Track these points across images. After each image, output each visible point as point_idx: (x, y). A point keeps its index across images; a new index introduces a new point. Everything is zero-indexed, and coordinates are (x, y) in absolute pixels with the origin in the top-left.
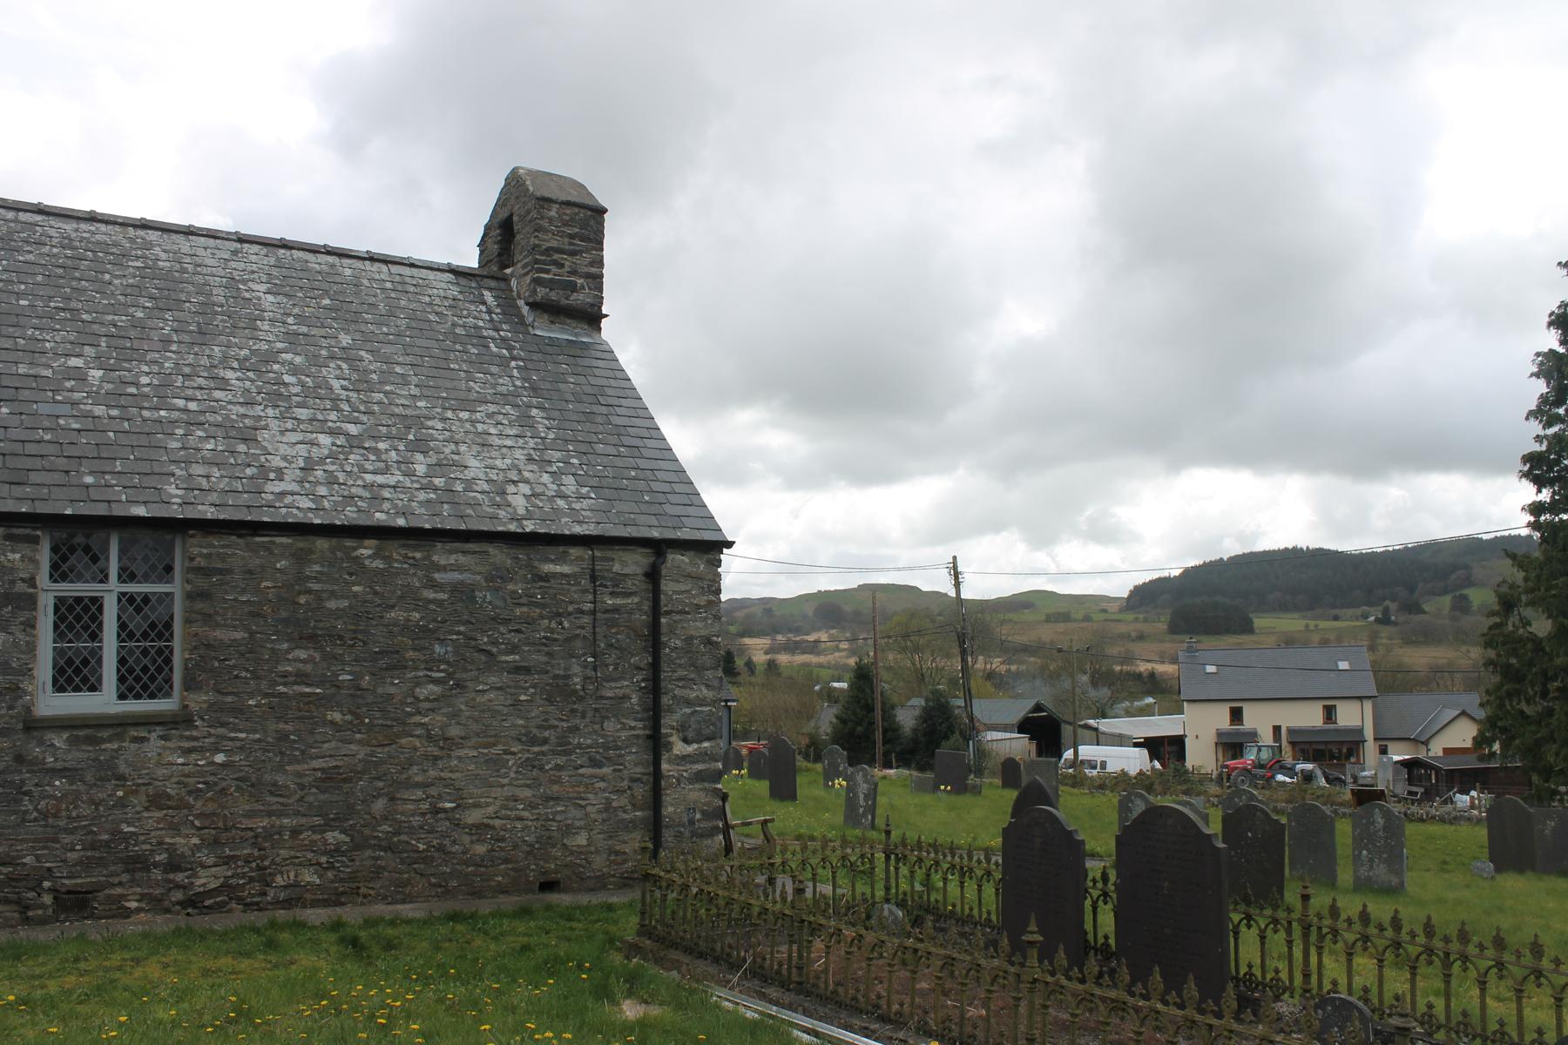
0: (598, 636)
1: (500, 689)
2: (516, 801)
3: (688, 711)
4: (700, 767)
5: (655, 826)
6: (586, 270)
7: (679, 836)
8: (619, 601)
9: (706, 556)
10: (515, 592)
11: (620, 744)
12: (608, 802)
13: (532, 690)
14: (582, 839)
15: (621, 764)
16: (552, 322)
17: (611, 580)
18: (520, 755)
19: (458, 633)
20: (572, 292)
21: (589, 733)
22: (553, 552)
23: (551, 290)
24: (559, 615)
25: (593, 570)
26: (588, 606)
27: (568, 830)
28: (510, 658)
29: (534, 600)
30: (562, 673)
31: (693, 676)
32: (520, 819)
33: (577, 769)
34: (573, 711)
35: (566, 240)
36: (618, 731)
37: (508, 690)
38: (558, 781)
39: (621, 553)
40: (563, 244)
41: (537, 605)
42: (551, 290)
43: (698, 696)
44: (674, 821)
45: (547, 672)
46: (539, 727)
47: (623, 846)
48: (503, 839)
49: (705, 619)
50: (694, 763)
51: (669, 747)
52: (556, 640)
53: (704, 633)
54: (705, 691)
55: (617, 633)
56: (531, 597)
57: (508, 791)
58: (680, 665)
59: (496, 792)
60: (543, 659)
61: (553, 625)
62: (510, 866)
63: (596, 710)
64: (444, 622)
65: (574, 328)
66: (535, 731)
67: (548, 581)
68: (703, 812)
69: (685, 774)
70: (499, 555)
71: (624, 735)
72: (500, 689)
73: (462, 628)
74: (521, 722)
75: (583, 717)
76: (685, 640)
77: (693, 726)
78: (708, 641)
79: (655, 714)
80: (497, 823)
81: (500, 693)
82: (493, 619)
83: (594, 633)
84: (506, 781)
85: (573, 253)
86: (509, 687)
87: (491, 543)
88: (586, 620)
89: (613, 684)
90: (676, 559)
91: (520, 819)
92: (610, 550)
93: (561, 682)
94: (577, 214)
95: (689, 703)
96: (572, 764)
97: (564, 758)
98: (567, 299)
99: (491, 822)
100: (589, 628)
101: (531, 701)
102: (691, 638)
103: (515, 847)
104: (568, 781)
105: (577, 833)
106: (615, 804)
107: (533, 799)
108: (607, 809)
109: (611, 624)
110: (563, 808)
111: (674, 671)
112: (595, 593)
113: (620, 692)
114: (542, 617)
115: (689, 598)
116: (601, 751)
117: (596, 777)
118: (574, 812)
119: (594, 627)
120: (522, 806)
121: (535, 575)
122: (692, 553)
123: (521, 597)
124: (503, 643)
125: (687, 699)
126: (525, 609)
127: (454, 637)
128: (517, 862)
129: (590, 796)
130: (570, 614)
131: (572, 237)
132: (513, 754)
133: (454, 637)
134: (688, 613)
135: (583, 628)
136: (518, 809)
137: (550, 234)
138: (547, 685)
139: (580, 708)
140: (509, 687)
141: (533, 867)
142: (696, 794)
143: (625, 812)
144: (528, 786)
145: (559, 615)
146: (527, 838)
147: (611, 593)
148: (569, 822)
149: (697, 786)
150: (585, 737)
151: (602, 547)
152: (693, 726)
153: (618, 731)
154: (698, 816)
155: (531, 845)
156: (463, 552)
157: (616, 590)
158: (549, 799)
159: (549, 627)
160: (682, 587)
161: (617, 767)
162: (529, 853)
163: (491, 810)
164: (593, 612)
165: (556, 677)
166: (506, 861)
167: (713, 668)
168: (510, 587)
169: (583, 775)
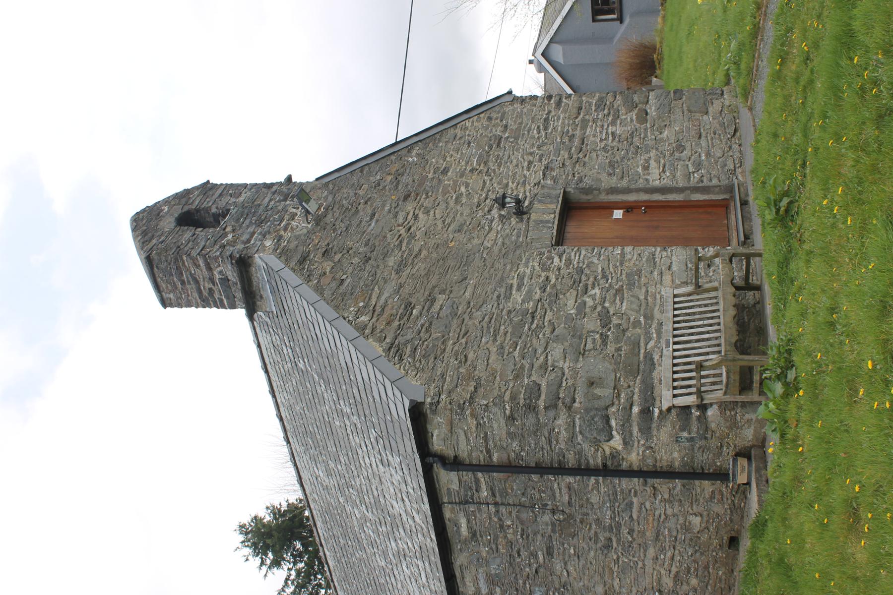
0: (517, 502)
1: (566, 564)
2: (657, 559)
3: (580, 437)
4: (635, 430)
5: (690, 474)
6: (204, 270)
7: (703, 449)
8: (483, 486)
9: (429, 416)
10: (488, 552)
11: (611, 492)
12: (663, 500)
13: (566, 545)
14: (696, 521)
15: (630, 491)
16: (261, 297)
17: (466, 491)
18: (620, 554)
19: (525, 583)
20: (228, 280)
21: (601, 512)
22: (450, 529)
23: (235, 297)
24: (501, 527)
25: (460, 503)
26: (492, 508)
27: (687, 528)
28: (541, 557)
29: (492, 541)
30: (550, 527)
31: (546, 433)
32: (673, 558)
33: (633, 519)
34: (582, 522)
35: (188, 286)
36: (599, 493)
37: (566, 559)
38: (642, 533)
39: (441, 483)
40: (192, 288)
41: (496, 538)
42: (235, 297)
43: (565, 430)
44: (687, 454)
45: (550, 536)
46: (596, 542)
47: (706, 492)
48: (689, 569)
49: (490, 420)
50: (631, 434)
51: (615, 455)
52: (523, 530)
53: (503, 422)
54: (559, 422)
55: (512, 489)
56: (490, 542)
57: (649, 563)
58: (535, 444)
59: (649, 569)
60: (539, 537)
61: (511, 531)
62: (711, 567)
63: (581, 506)
64: (517, 590)
65: (258, 279)
66: (599, 545)
67: (475, 531)
68: (682, 429)
69: (642, 442)
70: (460, 559)
71: (603, 489)
72: (566, 564)
73: (521, 582)
74: (592, 553)
75: (587, 514)
76: (512, 439)
77: (595, 435)
78: (511, 418)
79: (584, 471)
80: (674, 569)
81: (569, 563)
82: (511, 564)
83: (514, 505)
84: (640, 564)
85: (197, 282)
86: (564, 559)
87: (452, 563)
88: (503, 509)
89: (558, 494)
90: (437, 444)
91: (673, 558)
92: (440, 490)
93: (558, 528)
94: (162, 279)
95: (572, 438)
96: (628, 523)
97: (623, 527)
98: (236, 284)
99: (673, 573)
100: (509, 508)
101: (575, 547)
102: (509, 434)
103: (695, 561)
104: (643, 526)
105: (690, 523)
106: (666, 496)
107: (657, 549)
108: (670, 501)
109: (504, 493)
110: (667, 530)
111: (542, 448)
112: (480, 503)
113: (565, 490)
114: (506, 537)
115: (471, 433)
116: (617, 504)
117: (641, 508)
118: (671, 523)
119: (509, 505)
120: (662, 556)
121: (472, 538)
122: (428, 426)
123: (491, 548)
124: (529, 561)
125: (568, 439)
126: (500, 547)
127: (528, 585)
128: (708, 563)
129: (657, 513)
130: (500, 519)
131: (183, 283)
132: (618, 558)
133: (528, 585)
134: (486, 434)
135: (510, 513)
136: (665, 559)
137: (190, 298)
138: (560, 537)
139: (580, 517)
140: (564, 559)
141: (714, 554)
142: (663, 434)
143: (674, 488)
144: (645, 551)
145: (501, 527)
146: (690, 554)
147: (477, 491)
148: (679, 527)
149: (655, 433)
150: (605, 515)
151: (440, 498)
152: (595, 435)
153: (599, 493)
154: (685, 434)
155: (696, 552)
156: (463, 578)
157: (474, 487)
158: (657, 538)
159: (513, 534)
160: (462, 437)
161: (632, 494)
162: (702, 554)
163: (663, 572)
164: (496, 504)
165: (553, 531)
166: (706, 568)
167: (537, 414)
168: (484, 554)
169: (638, 517)
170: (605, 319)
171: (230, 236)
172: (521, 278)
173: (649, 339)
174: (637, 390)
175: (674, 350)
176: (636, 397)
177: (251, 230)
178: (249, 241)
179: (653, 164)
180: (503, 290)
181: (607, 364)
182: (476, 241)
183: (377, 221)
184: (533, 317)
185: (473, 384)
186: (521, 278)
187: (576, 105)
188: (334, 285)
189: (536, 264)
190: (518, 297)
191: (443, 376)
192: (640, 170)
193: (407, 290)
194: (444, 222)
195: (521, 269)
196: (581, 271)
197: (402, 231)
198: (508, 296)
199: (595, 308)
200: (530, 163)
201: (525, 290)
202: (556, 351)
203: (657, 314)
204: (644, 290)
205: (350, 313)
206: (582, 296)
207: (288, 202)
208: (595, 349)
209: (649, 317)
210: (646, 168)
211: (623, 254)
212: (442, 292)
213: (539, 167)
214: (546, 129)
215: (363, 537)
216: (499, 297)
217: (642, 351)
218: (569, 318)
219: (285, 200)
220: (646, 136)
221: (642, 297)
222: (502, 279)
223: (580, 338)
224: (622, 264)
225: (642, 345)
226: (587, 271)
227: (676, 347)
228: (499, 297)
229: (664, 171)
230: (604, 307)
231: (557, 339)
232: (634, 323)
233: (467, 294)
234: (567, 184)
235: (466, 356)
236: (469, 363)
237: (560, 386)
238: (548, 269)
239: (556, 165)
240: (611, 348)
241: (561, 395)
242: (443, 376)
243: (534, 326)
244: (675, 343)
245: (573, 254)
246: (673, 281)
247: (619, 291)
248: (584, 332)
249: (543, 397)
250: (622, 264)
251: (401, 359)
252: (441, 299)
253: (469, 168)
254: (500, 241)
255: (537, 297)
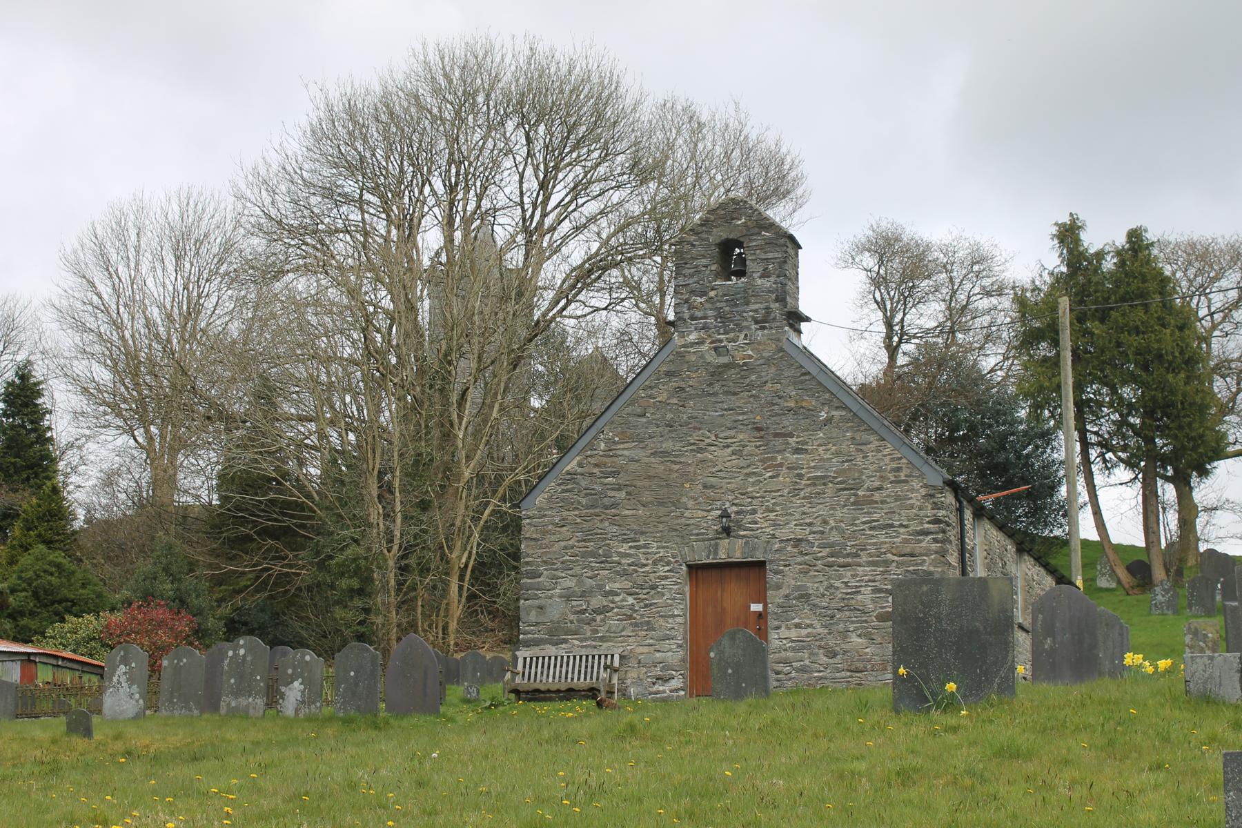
170: (603, 610)
171: (699, 300)
172: (645, 546)
173: (581, 640)
174: (536, 636)
175: (562, 657)
176: (531, 636)
177: (710, 313)
178: (693, 318)
179: (804, 632)
180: (632, 536)
181: (557, 616)
182: (691, 503)
183: (722, 415)
184: (602, 562)
185: (539, 536)
186: (645, 546)
187: (917, 551)
188: (639, 411)
189: (661, 555)
190: (624, 548)
191: (545, 516)
192: (797, 620)
193: (633, 467)
194: (721, 471)
195: (655, 545)
196: (654, 587)
197: (708, 441)
198: (624, 541)
199: (613, 603)
200: (810, 524)
201: (632, 551)
202: (570, 583)
203: (605, 645)
204: (631, 634)
205: (607, 434)
206: (625, 592)
207: (753, 327)
208: (572, 607)
209: (602, 639)
210: (798, 626)
211: (673, 616)
212: (628, 494)
213: (800, 533)
214: (871, 529)
215: (464, 496)
216: (625, 534)
217: (570, 637)
218: (601, 587)
219: (757, 322)
220: (852, 622)
221: (623, 633)
222: (643, 533)
223: (581, 596)
224: (662, 616)
225: (575, 636)
226: (653, 592)
227: (565, 658)
228: (625, 534)
229: (793, 641)
230: (613, 608)
231: (580, 583)
232: (597, 630)
233: (627, 512)
234: (772, 561)
235: (563, 526)
236: (558, 529)
237: (537, 590)
238: (655, 563)
239: (804, 547)
240: (573, 617)
241: (530, 592)
242: (545, 516)
243: (593, 564)
244: (568, 657)
245: (674, 579)
246: (642, 654)
247: (630, 617)
248: (588, 599)
249: (529, 581)
250: (662, 616)
251: (559, 485)
252: (623, 494)
253: (803, 472)
254: (692, 521)
255: (623, 561)
